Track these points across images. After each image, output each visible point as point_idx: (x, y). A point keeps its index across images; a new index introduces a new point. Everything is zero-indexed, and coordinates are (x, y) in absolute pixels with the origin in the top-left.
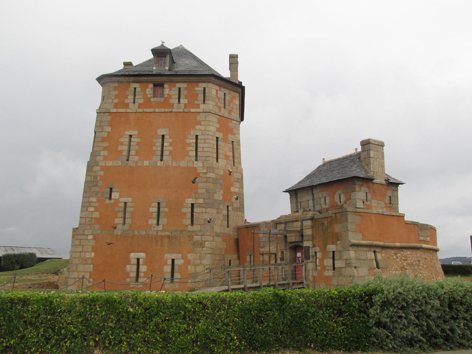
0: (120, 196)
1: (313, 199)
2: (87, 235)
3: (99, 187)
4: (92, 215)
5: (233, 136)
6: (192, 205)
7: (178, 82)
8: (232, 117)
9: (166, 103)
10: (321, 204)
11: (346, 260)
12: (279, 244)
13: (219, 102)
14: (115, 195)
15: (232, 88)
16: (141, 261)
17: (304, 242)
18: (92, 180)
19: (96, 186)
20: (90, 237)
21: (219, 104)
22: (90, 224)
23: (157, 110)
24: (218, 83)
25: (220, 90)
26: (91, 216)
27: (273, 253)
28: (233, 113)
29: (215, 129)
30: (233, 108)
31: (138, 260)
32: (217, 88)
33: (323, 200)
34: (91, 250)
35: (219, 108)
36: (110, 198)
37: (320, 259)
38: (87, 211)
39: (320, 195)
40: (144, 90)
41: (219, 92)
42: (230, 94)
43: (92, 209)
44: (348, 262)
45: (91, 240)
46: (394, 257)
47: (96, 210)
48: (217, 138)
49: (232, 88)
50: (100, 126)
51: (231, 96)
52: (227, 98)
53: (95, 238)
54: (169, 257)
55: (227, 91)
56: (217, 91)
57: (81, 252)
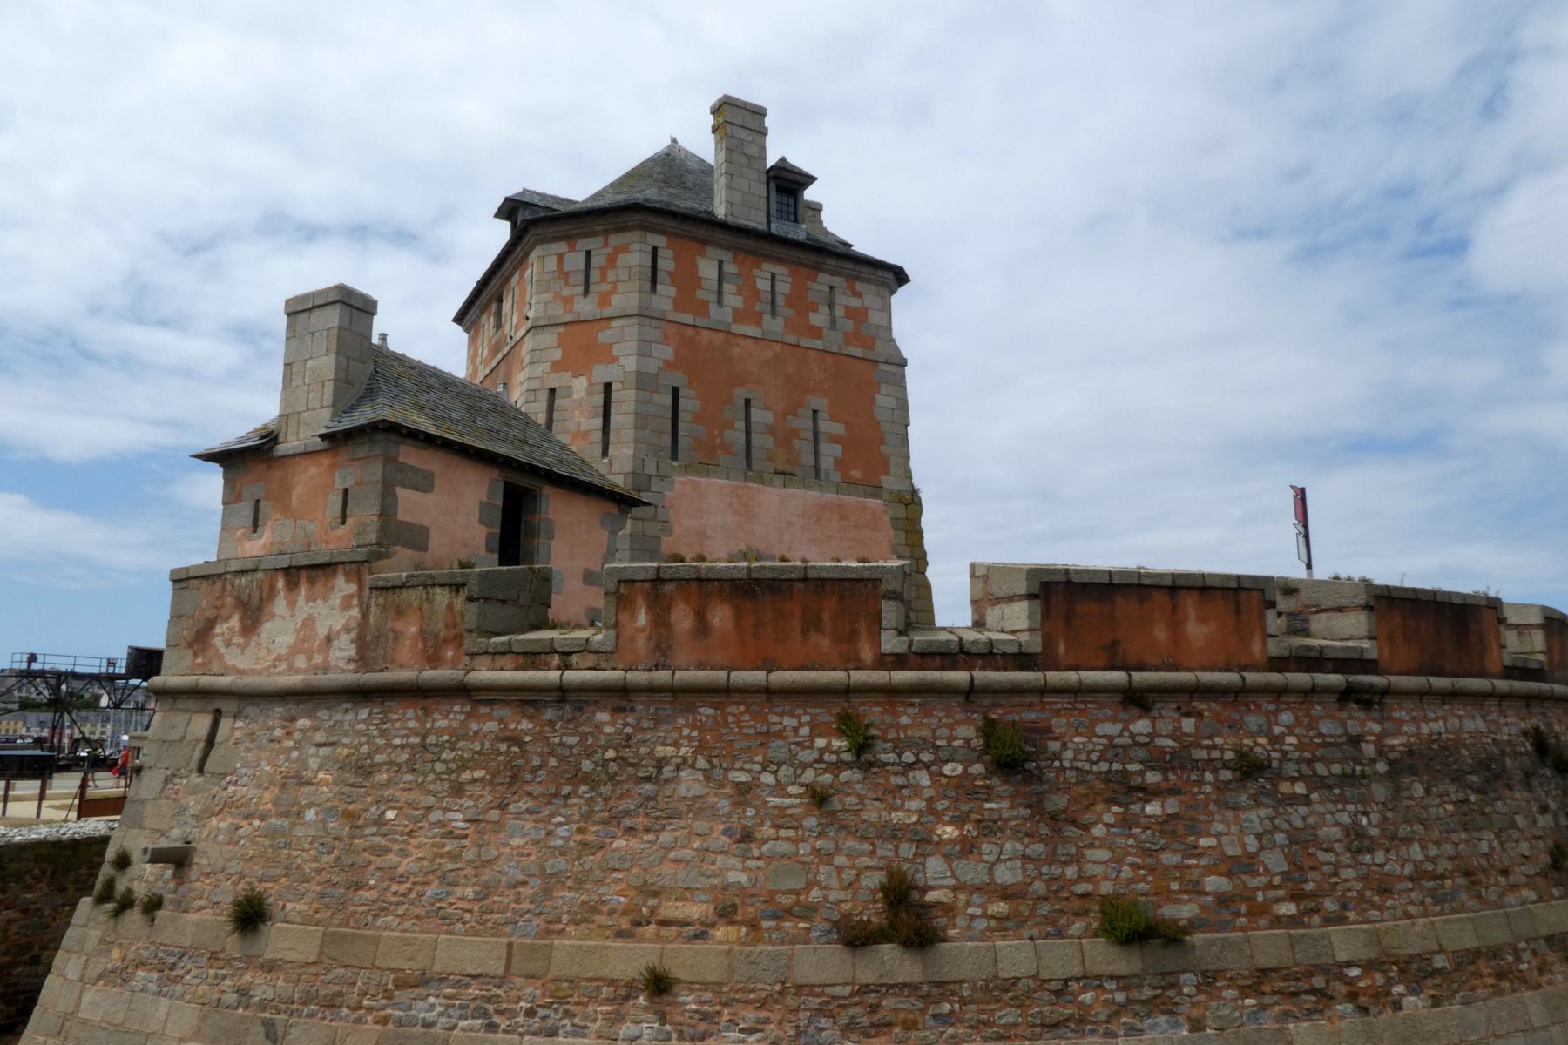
5: (610, 365)
8: (607, 312)
13: (567, 284)
15: (608, 227)
21: (566, 292)
24: (559, 234)
25: (572, 248)
28: (615, 300)
29: (546, 367)
30: (615, 283)
32: (562, 247)
35: (568, 301)
41: (567, 257)
42: (606, 244)
46: (278, 733)
48: (552, 391)
49: (608, 227)
51: (610, 250)
52: (597, 261)
55: (592, 243)
56: (560, 257)
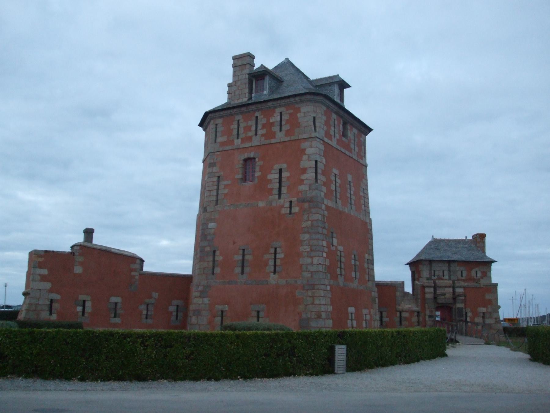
0: (338, 244)
1: (449, 271)
2: (327, 285)
3: (326, 229)
4: (326, 262)
6: (368, 259)
7: (354, 127)
9: (348, 147)
10: (458, 275)
11: (496, 318)
12: (426, 304)
14: (335, 241)
16: (353, 315)
17: (457, 304)
18: (322, 220)
19: (324, 228)
20: (328, 288)
22: (326, 273)
23: (347, 153)
26: (325, 264)
27: (415, 311)
31: (351, 314)
33: (459, 273)
34: (329, 303)
36: (333, 245)
37: (470, 318)
38: (322, 256)
39: (458, 268)
40: (339, 125)
43: (325, 255)
44: (497, 320)
45: (329, 292)
47: (327, 257)
50: (319, 154)
53: (331, 290)
54: (365, 311)
57: (325, 305)
